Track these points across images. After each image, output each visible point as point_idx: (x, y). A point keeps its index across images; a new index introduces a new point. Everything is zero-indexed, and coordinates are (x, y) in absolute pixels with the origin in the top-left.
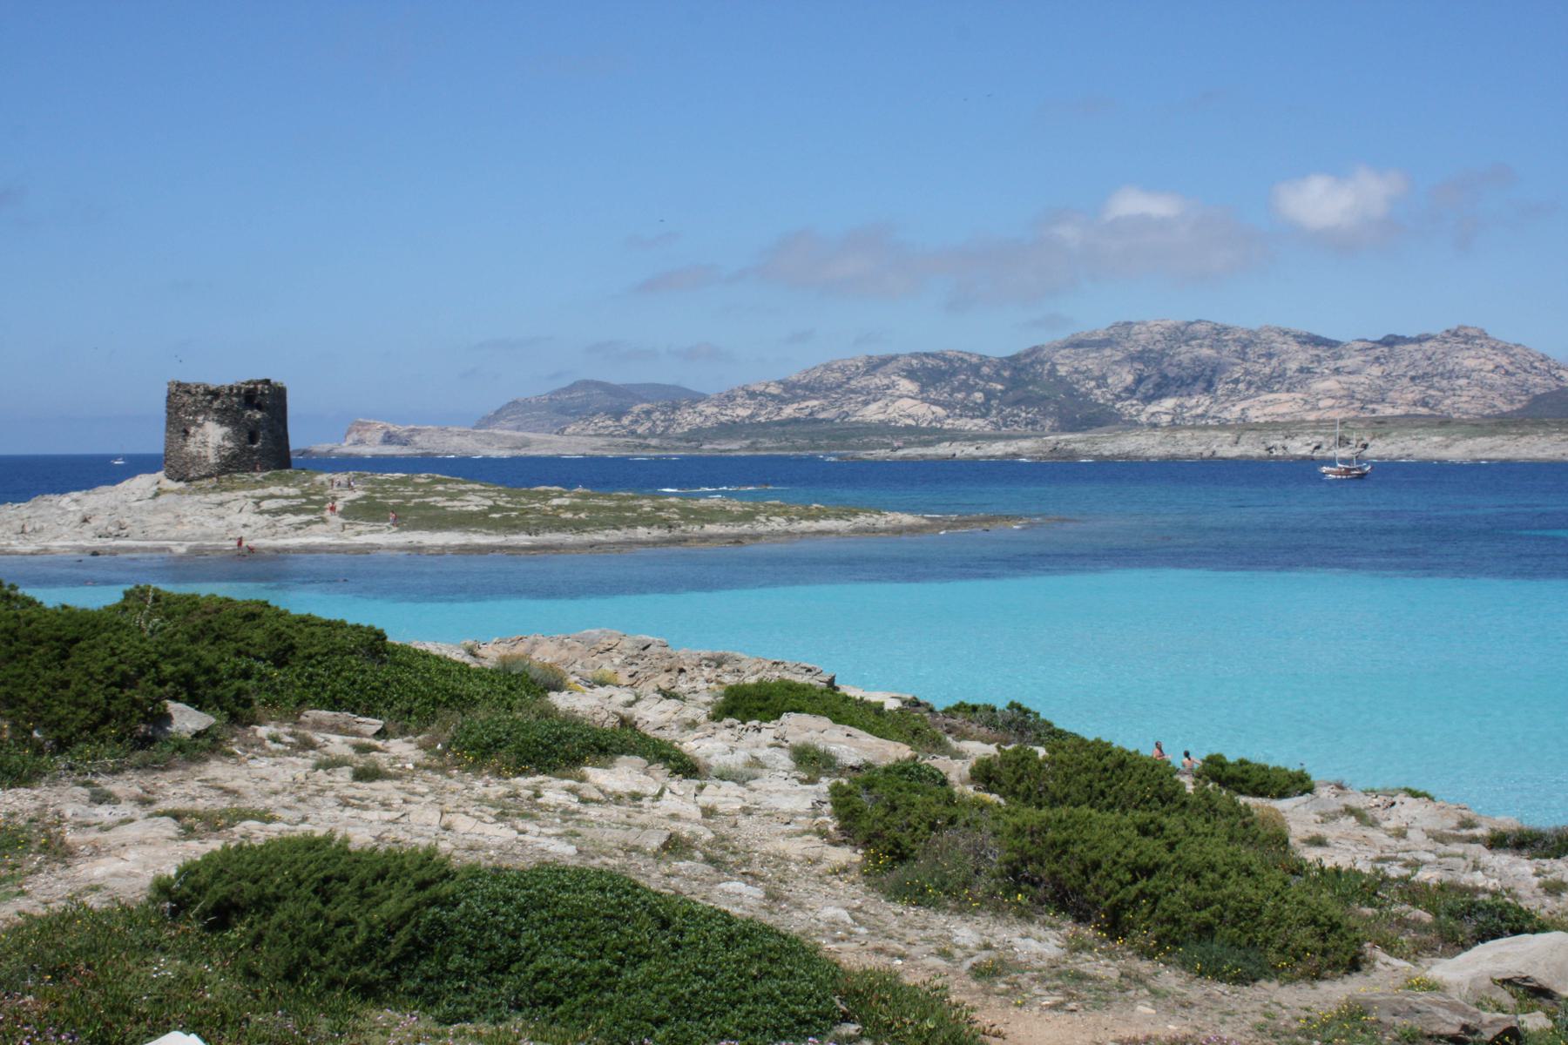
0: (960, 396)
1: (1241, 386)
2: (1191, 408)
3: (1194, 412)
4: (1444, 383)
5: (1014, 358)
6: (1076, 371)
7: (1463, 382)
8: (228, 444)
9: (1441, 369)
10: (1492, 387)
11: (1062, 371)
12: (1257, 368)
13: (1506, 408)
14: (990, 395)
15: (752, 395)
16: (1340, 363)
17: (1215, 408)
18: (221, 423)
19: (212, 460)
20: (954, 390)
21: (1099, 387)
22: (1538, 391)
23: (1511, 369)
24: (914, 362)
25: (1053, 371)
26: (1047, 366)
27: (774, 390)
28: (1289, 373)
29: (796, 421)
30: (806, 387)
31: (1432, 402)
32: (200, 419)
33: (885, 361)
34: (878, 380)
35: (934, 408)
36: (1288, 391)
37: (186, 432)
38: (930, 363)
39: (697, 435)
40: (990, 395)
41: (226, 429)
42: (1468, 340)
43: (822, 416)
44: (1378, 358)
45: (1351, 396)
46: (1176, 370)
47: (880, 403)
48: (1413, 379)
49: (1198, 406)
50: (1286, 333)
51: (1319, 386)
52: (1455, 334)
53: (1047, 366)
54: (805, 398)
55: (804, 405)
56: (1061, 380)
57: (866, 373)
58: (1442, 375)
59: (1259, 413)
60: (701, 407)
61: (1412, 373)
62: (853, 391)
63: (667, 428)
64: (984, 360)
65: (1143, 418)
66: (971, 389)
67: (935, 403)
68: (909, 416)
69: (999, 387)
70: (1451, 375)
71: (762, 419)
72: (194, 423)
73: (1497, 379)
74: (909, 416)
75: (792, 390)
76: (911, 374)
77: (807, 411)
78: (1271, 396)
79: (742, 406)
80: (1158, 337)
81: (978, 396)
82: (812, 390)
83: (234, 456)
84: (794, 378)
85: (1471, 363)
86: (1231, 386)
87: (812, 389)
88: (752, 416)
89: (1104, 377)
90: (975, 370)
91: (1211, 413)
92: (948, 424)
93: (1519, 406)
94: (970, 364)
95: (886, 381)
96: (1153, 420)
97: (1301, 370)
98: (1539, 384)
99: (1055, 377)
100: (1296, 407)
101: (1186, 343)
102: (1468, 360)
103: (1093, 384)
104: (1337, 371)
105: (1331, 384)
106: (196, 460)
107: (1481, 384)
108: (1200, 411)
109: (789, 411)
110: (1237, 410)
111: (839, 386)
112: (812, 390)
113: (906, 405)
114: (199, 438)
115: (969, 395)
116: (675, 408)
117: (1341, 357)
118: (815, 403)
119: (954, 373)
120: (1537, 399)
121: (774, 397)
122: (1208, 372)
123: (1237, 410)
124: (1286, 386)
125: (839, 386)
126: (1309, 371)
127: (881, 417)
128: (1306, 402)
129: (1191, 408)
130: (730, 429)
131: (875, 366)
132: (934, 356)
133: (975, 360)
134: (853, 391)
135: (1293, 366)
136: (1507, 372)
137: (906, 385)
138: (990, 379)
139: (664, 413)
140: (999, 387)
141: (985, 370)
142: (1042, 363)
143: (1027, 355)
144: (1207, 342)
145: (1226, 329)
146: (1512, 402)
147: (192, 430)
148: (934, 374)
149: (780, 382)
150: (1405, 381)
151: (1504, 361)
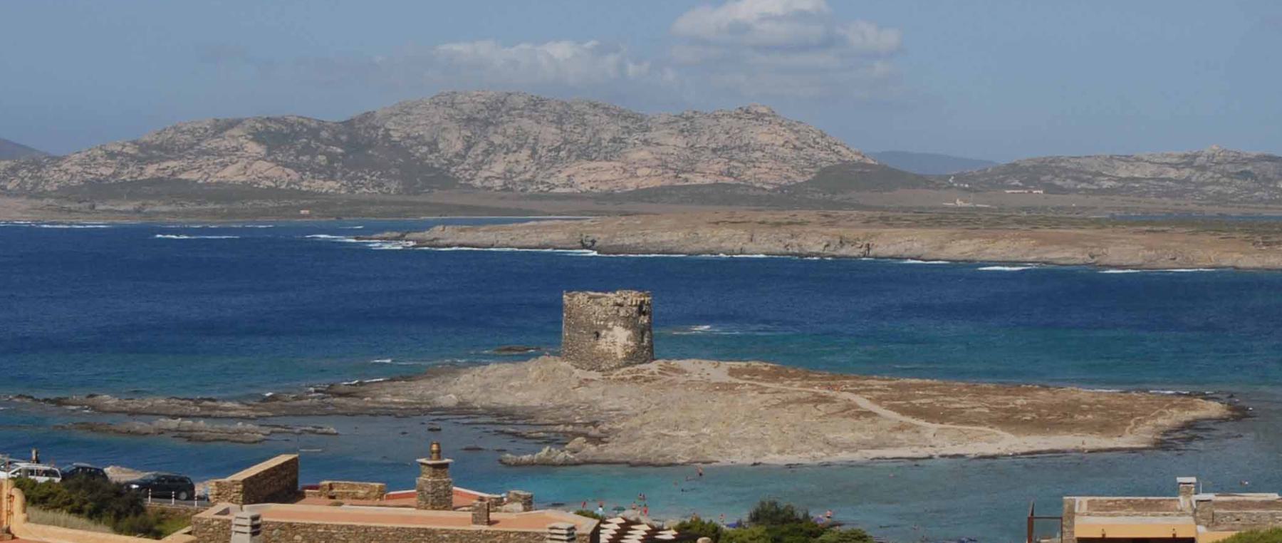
0: (305, 158)
1: (563, 154)
2: (520, 174)
3: (522, 177)
4: (743, 155)
5: (349, 123)
6: (408, 137)
7: (758, 154)
8: (631, 343)
9: (738, 142)
10: (784, 160)
11: (396, 136)
12: (575, 137)
13: (800, 180)
14: (332, 158)
15: (112, 155)
16: (648, 135)
17: (542, 174)
18: (626, 327)
19: (620, 357)
20: (299, 154)
21: (431, 152)
22: (824, 164)
23: (798, 144)
24: (259, 125)
25: (387, 135)
26: (381, 132)
27: (130, 150)
28: (604, 143)
29: (160, 180)
30: (159, 147)
31: (736, 172)
32: (610, 324)
33: (231, 124)
34: (225, 143)
35: (288, 170)
36: (606, 159)
37: (598, 335)
38: (274, 127)
39: (67, 192)
40: (332, 158)
41: (629, 332)
42: (759, 117)
43: (184, 176)
44: (682, 131)
45: (664, 165)
46: (501, 138)
47: (239, 165)
48: (714, 150)
49: (525, 172)
50: (595, 106)
51: (636, 155)
52: (747, 112)
53: (381, 132)
54: (163, 160)
55: (164, 165)
56: (395, 146)
57: (214, 135)
58: (740, 147)
59: (584, 180)
60: (65, 166)
61: (714, 146)
62: (204, 153)
63: (36, 185)
64: (320, 122)
65: (478, 183)
66: (313, 153)
67: (286, 165)
68: (267, 178)
69: (339, 150)
70: (746, 148)
71: (126, 177)
72: (605, 327)
73: (787, 152)
74: (267, 178)
75: (147, 152)
76: (257, 137)
77: (169, 172)
78: (593, 165)
79: (105, 165)
80: (481, 107)
81: (322, 159)
82: (166, 150)
83: (634, 352)
84: (147, 139)
85: (764, 139)
86: (553, 154)
87: (166, 150)
88: (114, 175)
89: (435, 143)
90: (314, 133)
91: (539, 179)
92: (305, 186)
93: (809, 177)
94: (310, 129)
95: (234, 144)
96: (486, 184)
97: (614, 140)
98: (825, 158)
99: (390, 142)
100: (616, 176)
101: (507, 113)
102: (761, 135)
103: (425, 149)
104: (646, 142)
105: (644, 154)
106: (607, 356)
107: (775, 158)
108: (528, 176)
109: (150, 171)
110: (563, 176)
111: (191, 147)
112: (166, 150)
113: (251, 167)
114: (609, 339)
115: (313, 157)
116: (40, 166)
117: (648, 129)
118: (172, 164)
119: (297, 135)
120: (824, 171)
121: (133, 157)
122: (531, 140)
123: (563, 176)
124: (602, 156)
125: (191, 147)
126: (621, 140)
127: (243, 179)
128: (625, 171)
129: (520, 174)
130: (99, 190)
131: (221, 128)
132: (277, 121)
133: (314, 124)
134: (204, 153)
135: (607, 136)
136: (795, 147)
137: (254, 148)
138: (328, 143)
139: (29, 171)
140: (339, 150)
141: (324, 134)
142: (376, 128)
143: (361, 120)
144: (526, 113)
145: (542, 101)
146: (803, 174)
147: (603, 333)
148: (278, 137)
149: (135, 143)
150: (708, 152)
151: (793, 137)
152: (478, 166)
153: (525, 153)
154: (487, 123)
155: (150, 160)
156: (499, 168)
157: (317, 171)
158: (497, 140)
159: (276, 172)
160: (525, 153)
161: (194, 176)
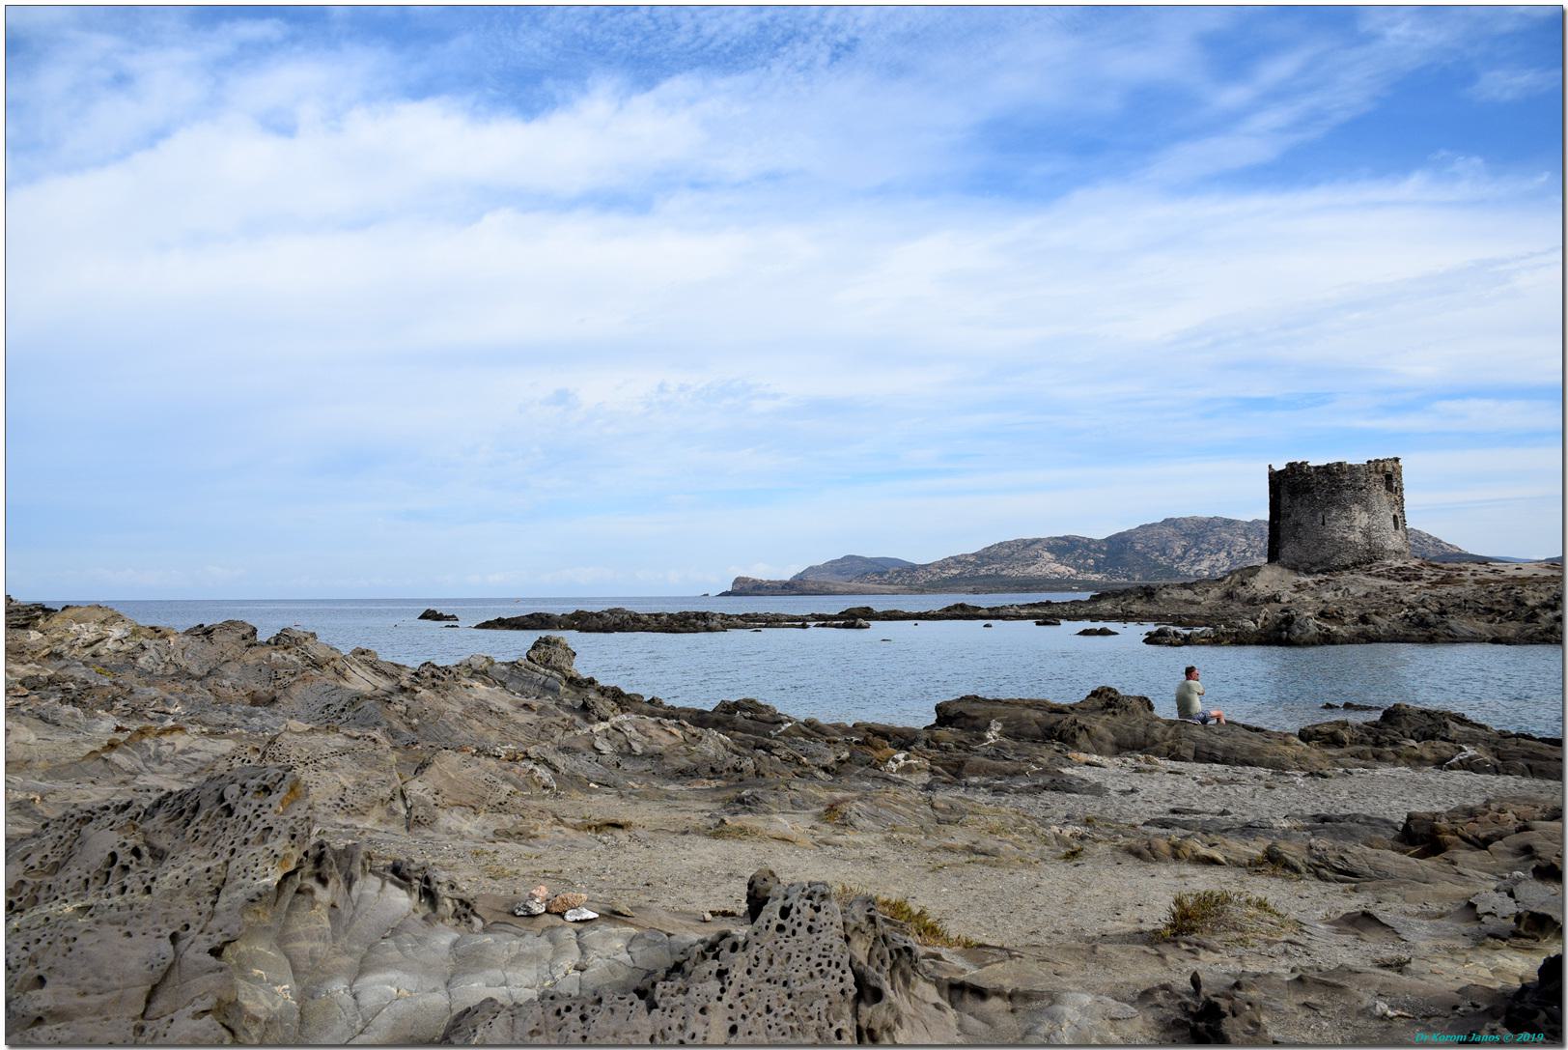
11: (1138, 547)
56: (1137, 553)
66: (1086, 558)
76: (1050, 550)
81: (1091, 562)
92: (1080, 577)
109: (983, 571)
137: (1047, 555)
138: (1095, 551)
142: (1125, 542)
152: (1193, 563)
153: (1223, 554)
154: (1197, 536)
155: (983, 565)
156: (1206, 564)
157: (1087, 570)
158: (1205, 546)
159: (1063, 569)
160: (1223, 554)
161: (1014, 573)
